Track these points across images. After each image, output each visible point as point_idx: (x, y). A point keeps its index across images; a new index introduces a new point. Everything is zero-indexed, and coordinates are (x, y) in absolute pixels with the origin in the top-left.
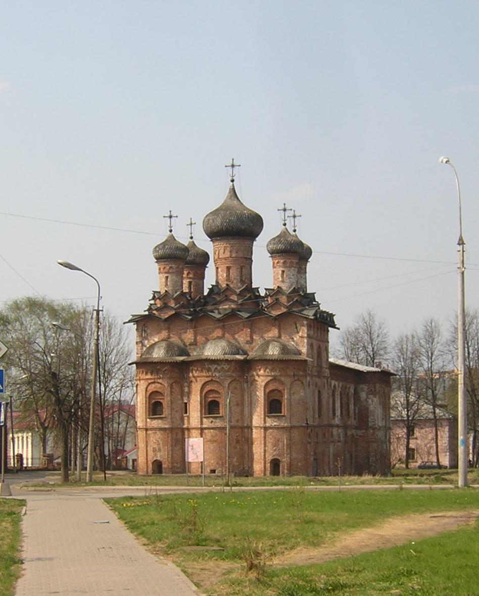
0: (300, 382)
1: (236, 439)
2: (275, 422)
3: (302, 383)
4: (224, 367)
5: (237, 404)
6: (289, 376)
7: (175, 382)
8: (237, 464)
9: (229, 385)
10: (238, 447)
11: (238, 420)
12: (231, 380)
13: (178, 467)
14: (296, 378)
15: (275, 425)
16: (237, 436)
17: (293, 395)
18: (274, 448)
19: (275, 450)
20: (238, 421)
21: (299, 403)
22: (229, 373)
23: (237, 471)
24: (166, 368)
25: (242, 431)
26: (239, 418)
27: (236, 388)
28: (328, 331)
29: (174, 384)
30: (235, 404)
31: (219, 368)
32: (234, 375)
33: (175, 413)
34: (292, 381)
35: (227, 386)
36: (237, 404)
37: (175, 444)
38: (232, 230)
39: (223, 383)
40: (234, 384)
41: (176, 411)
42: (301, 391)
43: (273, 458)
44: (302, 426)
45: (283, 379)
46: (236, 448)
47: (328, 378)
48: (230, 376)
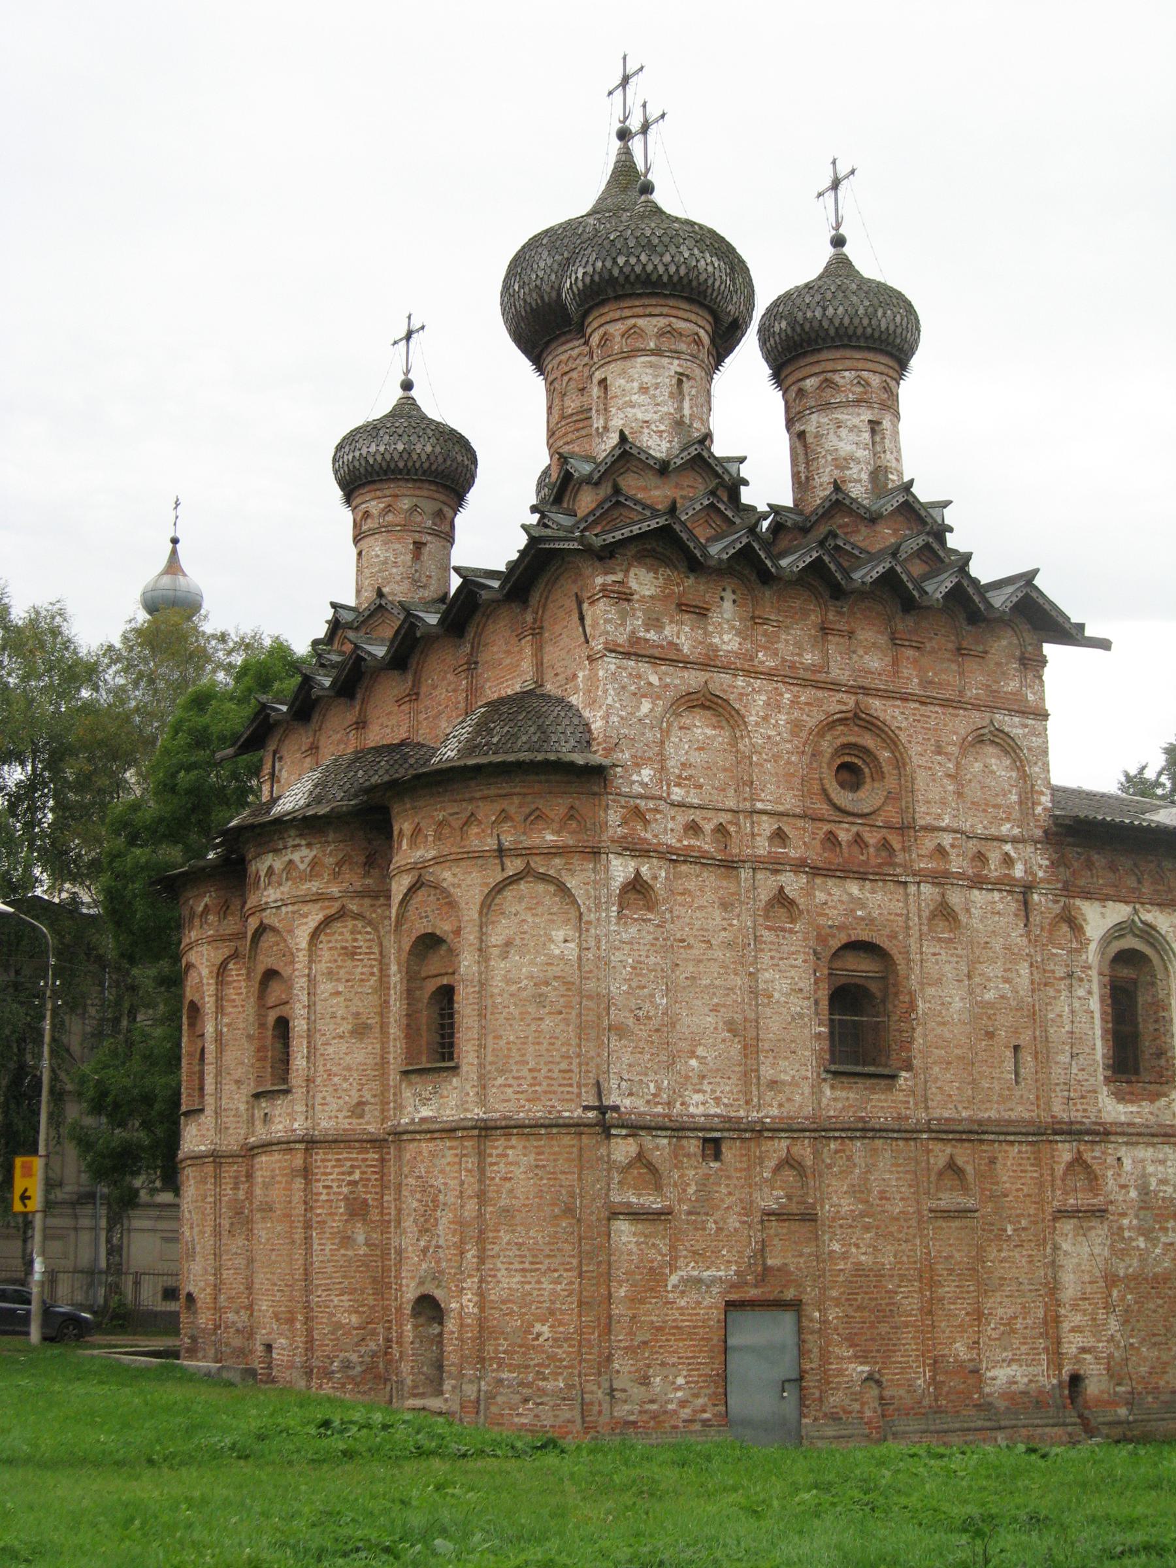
0: (541, 887)
1: (346, 1198)
2: (425, 1101)
3: (563, 890)
4: (296, 857)
5: (360, 1031)
6: (477, 856)
7: (235, 955)
8: (354, 1319)
9: (315, 935)
10: (361, 1239)
11: (360, 1104)
12: (320, 917)
13: (240, 1325)
14: (514, 866)
15: (423, 1120)
16: (350, 1183)
17: (504, 956)
18: (422, 1243)
19: (425, 1251)
20: (358, 1110)
21: (540, 1000)
22: (314, 886)
23: (354, 1357)
24: (207, 899)
25: (382, 1160)
26: (368, 1096)
27: (351, 953)
28: (1043, 662)
29: (231, 966)
30: (346, 1027)
31: (278, 864)
32: (335, 890)
33: (234, 1087)
34: (492, 882)
35: (304, 944)
36: (360, 1031)
37: (232, 1224)
38: (542, 298)
39: (291, 931)
40: (342, 933)
41: (238, 1082)
42: (558, 935)
43: (418, 1293)
44: (576, 1127)
45: (447, 876)
46: (346, 1240)
47: (1027, 888)
48: (318, 898)
